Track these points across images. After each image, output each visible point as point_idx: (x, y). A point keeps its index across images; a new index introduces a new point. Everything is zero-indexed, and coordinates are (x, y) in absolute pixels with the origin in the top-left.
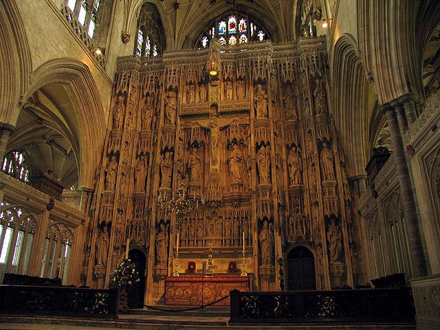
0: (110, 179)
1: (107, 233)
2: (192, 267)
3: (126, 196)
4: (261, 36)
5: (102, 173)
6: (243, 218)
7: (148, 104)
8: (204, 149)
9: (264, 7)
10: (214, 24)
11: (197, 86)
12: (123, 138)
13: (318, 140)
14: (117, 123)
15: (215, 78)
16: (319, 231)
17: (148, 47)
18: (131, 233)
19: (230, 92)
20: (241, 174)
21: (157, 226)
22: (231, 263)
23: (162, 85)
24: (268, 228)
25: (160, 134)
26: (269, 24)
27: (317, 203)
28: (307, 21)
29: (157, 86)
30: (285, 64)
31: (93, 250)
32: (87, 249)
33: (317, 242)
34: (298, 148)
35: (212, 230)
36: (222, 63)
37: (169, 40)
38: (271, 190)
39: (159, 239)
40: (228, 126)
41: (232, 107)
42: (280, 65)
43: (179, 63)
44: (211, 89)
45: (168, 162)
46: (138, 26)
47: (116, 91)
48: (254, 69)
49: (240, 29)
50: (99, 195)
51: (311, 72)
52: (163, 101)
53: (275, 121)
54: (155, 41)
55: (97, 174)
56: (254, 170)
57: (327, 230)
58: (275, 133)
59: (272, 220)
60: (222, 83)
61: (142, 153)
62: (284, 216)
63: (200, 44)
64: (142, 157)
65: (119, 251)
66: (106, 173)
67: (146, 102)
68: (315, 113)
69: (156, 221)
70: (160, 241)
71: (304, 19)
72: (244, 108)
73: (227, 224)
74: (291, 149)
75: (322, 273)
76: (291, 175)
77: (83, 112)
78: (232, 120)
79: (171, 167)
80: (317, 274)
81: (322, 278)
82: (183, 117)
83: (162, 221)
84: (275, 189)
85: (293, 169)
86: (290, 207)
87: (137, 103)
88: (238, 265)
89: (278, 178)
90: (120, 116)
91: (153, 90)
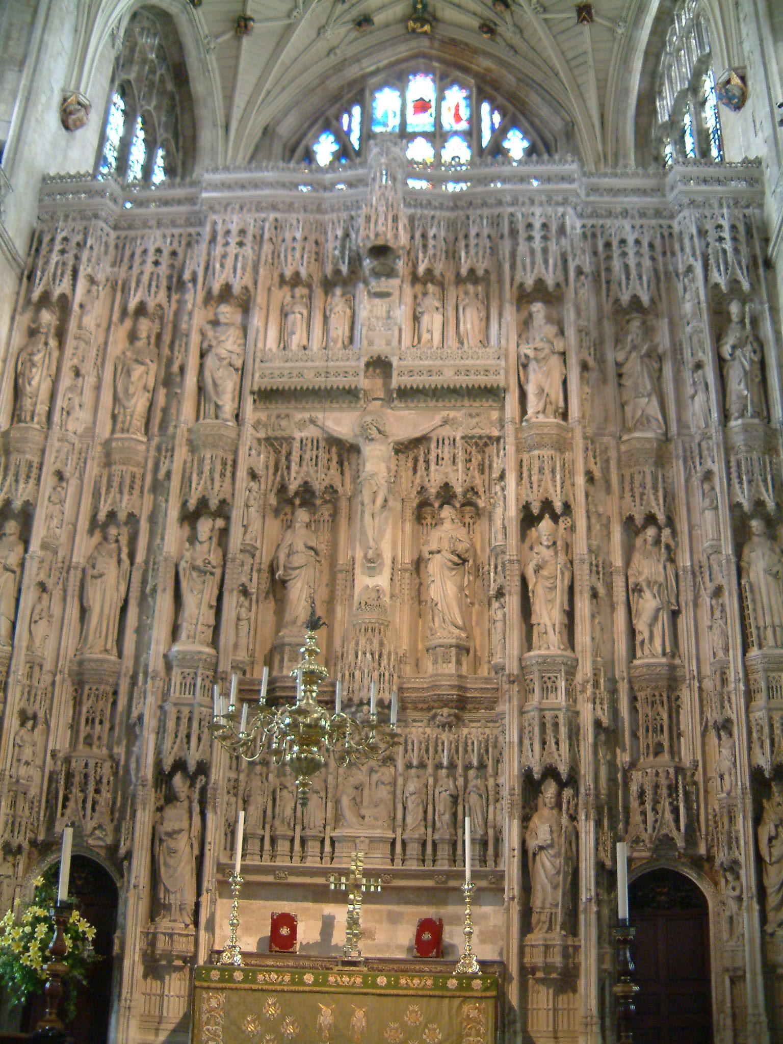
2: (285, 931)
3: (48, 666)
6: (468, 767)
7: (140, 344)
8: (334, 515)
9: (531, 54)
11: (318, 291)
12: (49, 459)
13: (735, 507)
14: (27, 403)
16: (732, 819)
17: (138, 153)
18: (66, 799)
19: (433, 321)
20: (466, 610)
21: (163, 778)
22: (426, 925)
23: (194, 280)
24: (559, 805)
25: (181, 453)
26: (544, 111)
27: (725, 726)
29: (176, 285)
30: (623, 242)
33: (722, 857)
34: (666, 532)
35: (356, 803)
36: (412, 219)
37: (208, 136)
38: (571, 673)
39: (168, 827)
42: (608, 245)
43: (259, 209)
44: (367, 308)
46: (113, 80)
47: (29, 291)
48: (523, 248)
52: (195, 338)
53: (590, 431)
56: (513, 602)
57: (758, 820)
59: (573, 781)
60: (408, 290)
61: (112, 515)
62: (612, 765)
63: (309, 156)
65: (22, 860)
67: (133, 337)
68: (725, 416)
69: (158, 763)
70: (170, 835)
71: (665, 106)
72: (481, 380)
73: (412, 787)
74: (638, 532)
75: (739, 964)
76: (641, 626)
78: (437, 420)
79: (218, 572)
81: (737, 979)
83: (180, 765)
84: (585, 670)
85: (648, 603)
86: (634, 735)
87: (101, 339)
88: (447, 929)
89: (598, 635)
91: (162, 294)
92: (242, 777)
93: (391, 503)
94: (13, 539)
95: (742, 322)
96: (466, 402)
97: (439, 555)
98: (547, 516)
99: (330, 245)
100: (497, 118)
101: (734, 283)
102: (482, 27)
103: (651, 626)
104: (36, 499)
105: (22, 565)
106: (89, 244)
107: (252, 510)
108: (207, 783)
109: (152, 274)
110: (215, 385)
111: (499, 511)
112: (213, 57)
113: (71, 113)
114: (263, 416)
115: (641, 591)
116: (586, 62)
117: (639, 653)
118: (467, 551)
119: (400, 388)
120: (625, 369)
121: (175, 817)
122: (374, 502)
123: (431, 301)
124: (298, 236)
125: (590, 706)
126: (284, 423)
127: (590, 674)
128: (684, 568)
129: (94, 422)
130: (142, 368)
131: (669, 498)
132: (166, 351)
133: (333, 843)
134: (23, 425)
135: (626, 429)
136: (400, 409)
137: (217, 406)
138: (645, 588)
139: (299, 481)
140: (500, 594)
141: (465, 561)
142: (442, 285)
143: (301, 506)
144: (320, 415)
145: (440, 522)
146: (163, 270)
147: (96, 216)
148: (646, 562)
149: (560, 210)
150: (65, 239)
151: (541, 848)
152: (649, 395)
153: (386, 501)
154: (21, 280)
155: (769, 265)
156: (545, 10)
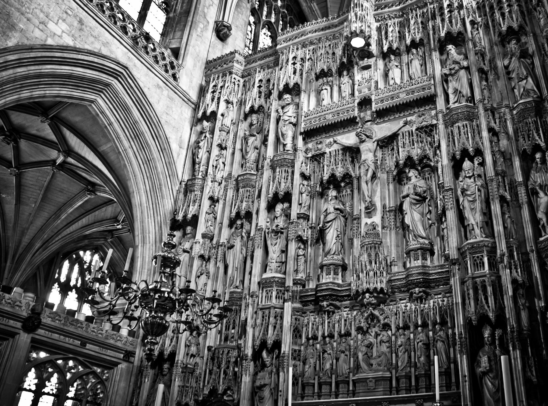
19: (395, 74)
38: (492, 251)
44: (358, 77)
58: (491, 130)
72: (422, 94)
78: (401, 123)
93: (379, 175)
96: (416, 110)
97: (408, 199)
98: (466, 159)
104: (199, 213)
107: (304, 195)
114: (310, 145)
115: (537, 193)
118: (425, 192)
119: (376, 110)
120: (510, 69)
122: (366, 176)
125: (508, 271)
126: (320, 146)
127: (505, 250)
130: (254, 138)
136: (380, 123)
138: (539, 190)
141: (424, 199)
148: (538, 175)
152: (526, 78)
153: (374, 173)
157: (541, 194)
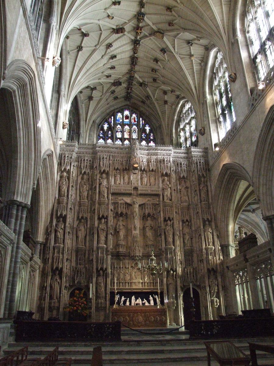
0: (60, 235)
1: (57, 277)
4: (147, 128)
5: (53, 231)
7: (85, 180)
10: (114, 114)
13: (203, 219)
15: (136, 168)
19: (145, 180)
23: (96, 167)
25: (97, 206)
26: (154, 121)
28: (185, 126)
29: (92, 167)
30: (181, 164)
31: (48, 289)
32: (42, 288)
33: (202, 285)
34: (190, 223)
37: (82, 123)
40: (144, 204)
41: (148, 191)
42: (178, 164)
43: (108, 152)
45: (102, 226)
49: (133, 121)
50: (51, 248)
51: (199, 173)
52: (98, 181)
54: (73, 123)
55: (49, 231)
56: (163, 237)
57: (209, 278)
60: (140, 173)
64: (83, 221)
66: (56, 231)
67: (82, 179)
69: (97, 269)
76: (186, 241)
77: (43, 184)
80: (201, 305)
82: (113, 194)
83: (102, 269)
85: (187, 237)
87: (76, 179)
90: (65, 188)
92: (112, 271)
94: (62, 222)
95: (204, 182)
99: (124, 162)
100: (143, 122)
101: (203, 175)
102: (142, 101)
103: (187, 241)
105: (65, 227)
106: (73, 157)
108: (107, 272)
109: (86, 165)
110: (103, 191)
111: (159, 219)
112: (84, 105)
113: (65, 126)
114: (113, 198)
116: (165, 113)
117: (185, 246)
120: (181, 191)
121: (101, 279)
123: (144, 175)
124: (118, 160)
126: (117, 199)
128: (193, 230)
129: (76, 197)
131: (190, 216)
132: (91, 183)
133: (131, 283)
134: (62, 198)
135: (182, 203)
137: (103, 195)
139: (120, 212)
140: (160, 235)
142: (146, 172)
143: (120, 216)
144: (124, 198)
145: (147, 220)
146: (88, 164)
147: (73, 151)
149: (169, 157)
150: (68, 156)
151: (170, 284)
154: (58, 165)
155: (209, 170)
156: (157, 100)
157: (187, 235)
